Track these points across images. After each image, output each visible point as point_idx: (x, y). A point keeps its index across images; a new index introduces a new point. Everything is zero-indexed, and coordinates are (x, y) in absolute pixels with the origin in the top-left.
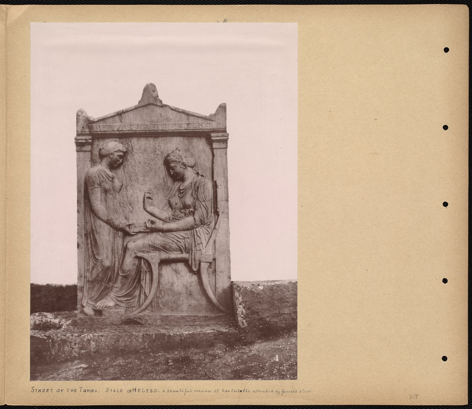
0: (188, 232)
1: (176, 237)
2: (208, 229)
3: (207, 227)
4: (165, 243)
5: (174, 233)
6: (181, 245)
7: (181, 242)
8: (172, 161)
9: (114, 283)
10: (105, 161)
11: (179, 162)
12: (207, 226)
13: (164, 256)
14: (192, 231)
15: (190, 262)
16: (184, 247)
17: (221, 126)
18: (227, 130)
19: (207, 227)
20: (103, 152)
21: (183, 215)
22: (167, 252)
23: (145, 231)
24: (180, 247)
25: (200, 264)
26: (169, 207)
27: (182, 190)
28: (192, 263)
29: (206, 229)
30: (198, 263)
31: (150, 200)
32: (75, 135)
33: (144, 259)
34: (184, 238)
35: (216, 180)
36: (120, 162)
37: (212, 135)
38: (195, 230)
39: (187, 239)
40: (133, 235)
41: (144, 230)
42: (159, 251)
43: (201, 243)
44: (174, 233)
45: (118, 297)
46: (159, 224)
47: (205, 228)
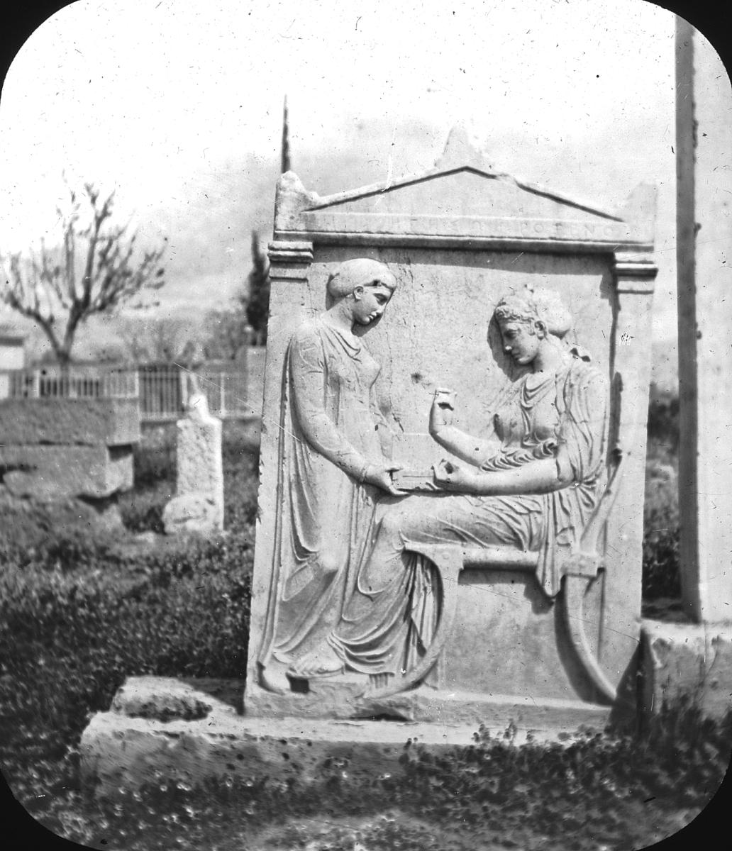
0: (538, 498)
1: (505, 507)
2: (590, 494)
4: (478, 521)
5: (510, 497)
6: (519, 530)
8: (511, 318)
13: (476, 553)
14: (550, 495)
15: (539, 574)
19: (588, 489)
20: (339, 284)
21: (530, 454)
22: (485, 544)
23: (431, 489)
24: (515, 534)
25: (564, 580)
27: (531, 391)
28: (544, 575)
30: (560, 577)
33: (423, 558)
34: (526, 511)
35: (619, 371)
37: (619, 256)
38: (556, 493)
39: (536, 514)
40: (399, 498)
41: (428, 487)
42: (462, 539)
44: (505, 498)
45: (353, 648)
46: (468, 474)
47: (584, 490)
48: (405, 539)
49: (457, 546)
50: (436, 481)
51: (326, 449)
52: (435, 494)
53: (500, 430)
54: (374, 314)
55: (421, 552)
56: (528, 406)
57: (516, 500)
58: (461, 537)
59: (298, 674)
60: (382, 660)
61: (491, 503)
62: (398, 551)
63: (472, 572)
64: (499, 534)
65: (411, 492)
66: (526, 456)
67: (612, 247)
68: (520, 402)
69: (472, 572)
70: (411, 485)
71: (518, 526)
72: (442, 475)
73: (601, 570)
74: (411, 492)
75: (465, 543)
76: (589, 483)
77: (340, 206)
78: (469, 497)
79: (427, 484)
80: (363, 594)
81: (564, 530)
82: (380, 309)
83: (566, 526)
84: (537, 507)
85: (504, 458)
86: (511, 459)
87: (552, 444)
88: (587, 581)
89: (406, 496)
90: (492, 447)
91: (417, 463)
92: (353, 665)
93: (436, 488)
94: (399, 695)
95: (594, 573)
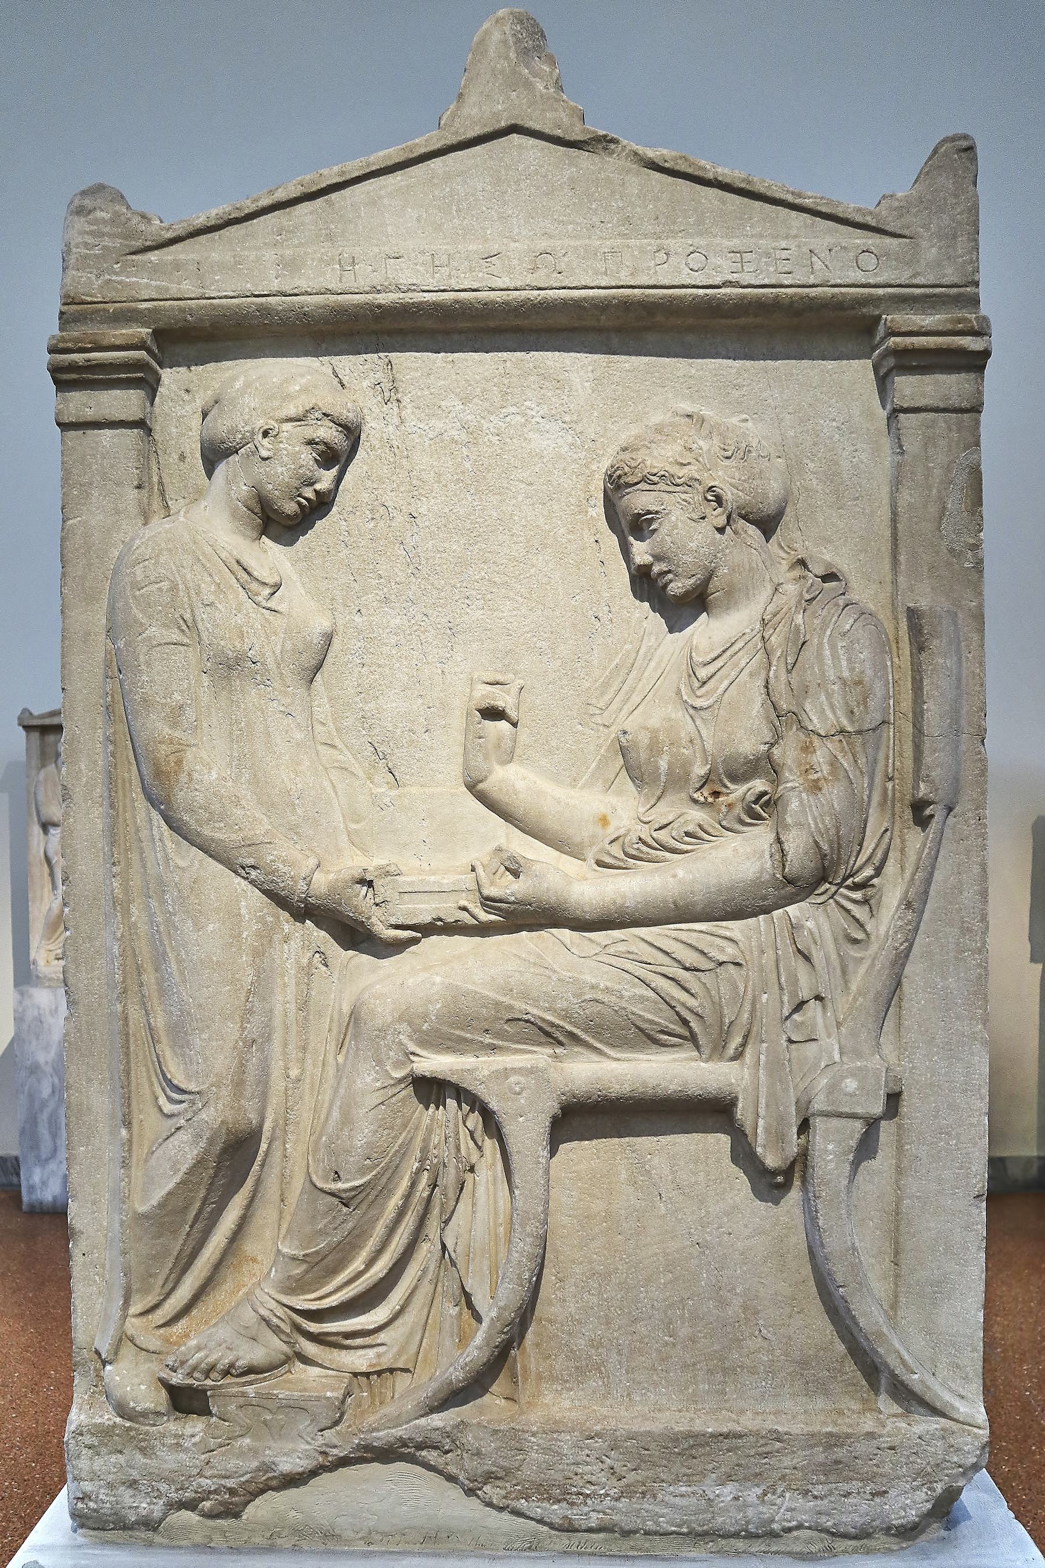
0: (734, 928)
3: (855, 901)
7: (695, 988)
8: (644, 479)
9: (283, 1231)
10: (233, 480)
11: (689, 483)
12: (857, 895)
16: (709, 1020)
17: (950, 274)
18: (983, 292)
19: (855, 901)
20: (221, 426)
24: (685, 1022)
25: (804, 1126)
26: (624, 770)
29: (848, 911)
31: (503, 724)
32: (53, 328)
34: (712, 965)
36: (318, 487)
40: (397, 947)
43: (818, 998)
48: (412, 1047)
49: (540, 1056)
50: (488, 902)
51: (207, 831)
52: (483, 930)
53: (635, 765)
54: (309, 493)
55: (454, 1079)
56: (698, 703)
57: (675, 934)
58: (548, 1035)
59: (177, 1379)
60: (382, 1337)
61: (622, 947)
62: (400, 1081)
63: (581, 1117)
64: (645, 1026)
65: (428, 929)
66: (700, 826)
67: (876, 301)
68: (679, 692)
69: (581, 1117)
70: (424, 911)
71: (692, 1002)
72: (506, 887)
73: (894, 1099)
74: (428, 929)
75: (559, 1050)
76: (856, 887)
77: (216, 235)
78: (565, 934)
79: (464, 909)
80: (321, 1190)
81: (799, 1006)
82: (326, 479)
83: (805, 993)
84: (730, 952)
85: (643, 837)
86: (663, 836)
87: (764, 794)
88: (858, 1127)
89: (414, 941)
90: (625, 810)
91: (437, 858)
92: (310, 1349)
93: (485, 917)
94: (423, 1421)
95: (877, 1108)
